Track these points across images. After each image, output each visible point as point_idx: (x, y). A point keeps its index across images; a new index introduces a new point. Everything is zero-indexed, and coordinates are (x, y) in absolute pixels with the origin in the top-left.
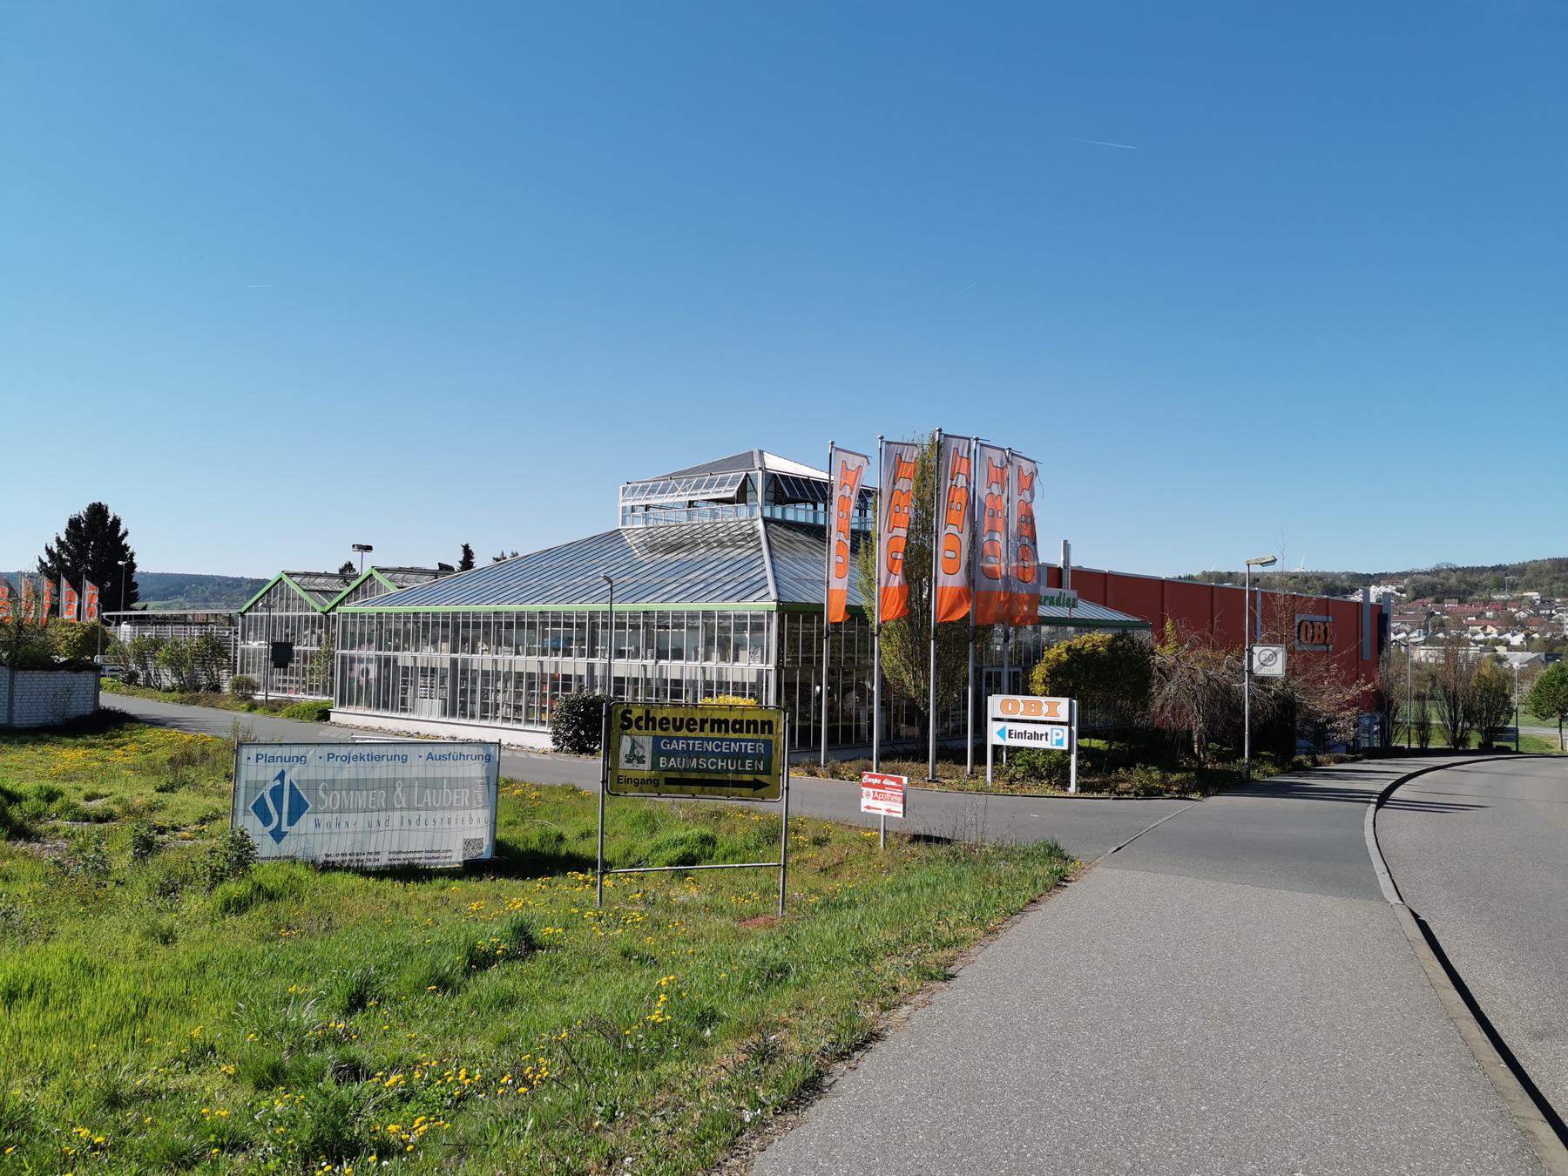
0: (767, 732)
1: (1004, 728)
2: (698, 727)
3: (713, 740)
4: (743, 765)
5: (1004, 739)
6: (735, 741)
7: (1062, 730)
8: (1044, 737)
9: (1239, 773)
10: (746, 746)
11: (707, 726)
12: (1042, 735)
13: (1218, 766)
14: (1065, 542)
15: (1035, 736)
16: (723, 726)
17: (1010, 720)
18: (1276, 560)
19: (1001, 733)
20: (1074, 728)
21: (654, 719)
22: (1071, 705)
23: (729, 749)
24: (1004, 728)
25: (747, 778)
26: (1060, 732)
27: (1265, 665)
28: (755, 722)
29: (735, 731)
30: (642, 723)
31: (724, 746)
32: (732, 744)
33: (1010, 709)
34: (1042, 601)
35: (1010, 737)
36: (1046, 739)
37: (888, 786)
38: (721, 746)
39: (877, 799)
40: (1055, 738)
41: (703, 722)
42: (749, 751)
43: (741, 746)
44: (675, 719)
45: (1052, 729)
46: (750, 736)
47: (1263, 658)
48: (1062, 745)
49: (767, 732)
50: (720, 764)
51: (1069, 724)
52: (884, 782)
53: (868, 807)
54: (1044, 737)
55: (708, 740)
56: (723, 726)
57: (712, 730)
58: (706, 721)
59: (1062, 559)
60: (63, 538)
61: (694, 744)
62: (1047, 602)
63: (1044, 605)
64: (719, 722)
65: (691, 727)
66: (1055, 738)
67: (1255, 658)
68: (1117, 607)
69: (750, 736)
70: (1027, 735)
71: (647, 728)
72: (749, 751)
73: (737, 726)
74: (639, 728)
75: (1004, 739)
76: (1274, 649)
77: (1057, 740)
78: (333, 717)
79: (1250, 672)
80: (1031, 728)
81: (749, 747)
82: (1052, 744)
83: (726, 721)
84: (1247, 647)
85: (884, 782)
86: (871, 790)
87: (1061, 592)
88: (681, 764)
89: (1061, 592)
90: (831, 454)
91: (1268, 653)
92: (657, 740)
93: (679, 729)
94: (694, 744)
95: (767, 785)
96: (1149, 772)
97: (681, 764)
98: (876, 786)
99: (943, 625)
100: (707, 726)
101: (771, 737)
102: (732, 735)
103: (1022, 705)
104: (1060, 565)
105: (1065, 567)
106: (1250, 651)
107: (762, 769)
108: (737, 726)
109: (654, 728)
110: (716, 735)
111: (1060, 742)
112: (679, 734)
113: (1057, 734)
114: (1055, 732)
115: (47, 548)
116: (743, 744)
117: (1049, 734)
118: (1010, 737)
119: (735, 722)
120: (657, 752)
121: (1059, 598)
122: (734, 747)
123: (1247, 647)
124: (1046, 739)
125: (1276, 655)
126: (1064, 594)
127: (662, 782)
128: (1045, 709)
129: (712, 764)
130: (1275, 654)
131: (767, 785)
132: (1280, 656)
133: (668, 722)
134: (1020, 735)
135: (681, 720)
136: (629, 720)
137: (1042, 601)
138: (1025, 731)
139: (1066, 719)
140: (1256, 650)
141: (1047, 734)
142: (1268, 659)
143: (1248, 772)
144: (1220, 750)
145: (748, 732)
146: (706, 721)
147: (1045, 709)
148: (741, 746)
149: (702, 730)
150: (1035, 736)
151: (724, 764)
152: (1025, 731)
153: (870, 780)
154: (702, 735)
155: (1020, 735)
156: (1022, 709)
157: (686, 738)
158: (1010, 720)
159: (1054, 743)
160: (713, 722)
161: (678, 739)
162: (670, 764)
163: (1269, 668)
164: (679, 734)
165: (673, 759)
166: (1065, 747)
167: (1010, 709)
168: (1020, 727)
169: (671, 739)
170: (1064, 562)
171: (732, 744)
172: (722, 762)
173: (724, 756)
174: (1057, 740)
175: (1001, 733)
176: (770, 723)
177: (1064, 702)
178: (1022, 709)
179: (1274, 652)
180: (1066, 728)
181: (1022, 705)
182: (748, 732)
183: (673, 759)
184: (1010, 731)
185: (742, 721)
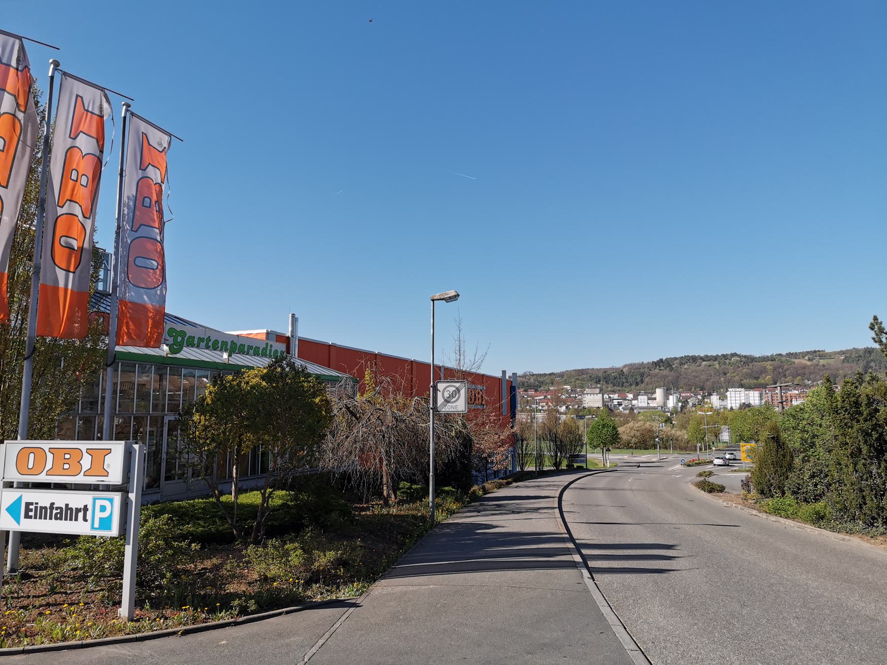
1: (21, 496)
5: (19, 523)
7: (111, 501)
8: (81, 515)
9: (423, 518)
12: (78, 510)
13: (405, 510)
14: (293, 315)
15: (68, 513)
17: (25, 486)
18: (458, 295)
20: (132, 496)
22: (128, 455)
24: (20, 498)
26: (107, 504)
27: (449, 402)
33: (30, 466)
34: (246, 350)
35: (27, 516)
36: (85, 520)
45: (95, 499)
47: (446, 395)
48: (109, 528)
54: (81, 515)
59: (290, 329)
62: (251, 352)
63: (247, 354)
66: (99, 515)
67: (439, 394)
70: (54, 512)
75: (19, 523)
76: (457, 385)
77: (100, 518)
79: (435, 409)
80: (61, 499)
82: (93, 528)
84: (432, 384)
87: (267, 344)
89: (267, 344)
91: (452, 389)
96: (286, 554)
103: (50, 457)
104: (289, 334)
105: (292, 336)
106: (435, 389)
114: (99, 503)
117: (90, 507)
121: (265, 349)
123: (432, 384)
124: (85, 520)
125: (459, 391)
126: (271, 346)
128: (86, 462)
130: (458, 390)
132: (463, 392)
134: (43, 513)
137: (246, 350)
138: (52, 504)
139: (115, 477)
140: (441, 386)
141: (86, 509)
142: (452, 396)
143: (433, 515)
144: (410, 488)
147: (86, 462)
150: (68, 513)
152: (52, 504)
155: (43, 513)
156: (49, 465)
158: (25, 486)
159: (96, 525)
163: (453, 405)
166: (114, 532)
167: (30, 466)
168: (43, 498)
170: (292, 332)
174: (100, 518)
177: (118, 448)
178: (49, 465)
179: (457, 388)
180: (117, 497)
181: (50, 457)
184: (28, 504)
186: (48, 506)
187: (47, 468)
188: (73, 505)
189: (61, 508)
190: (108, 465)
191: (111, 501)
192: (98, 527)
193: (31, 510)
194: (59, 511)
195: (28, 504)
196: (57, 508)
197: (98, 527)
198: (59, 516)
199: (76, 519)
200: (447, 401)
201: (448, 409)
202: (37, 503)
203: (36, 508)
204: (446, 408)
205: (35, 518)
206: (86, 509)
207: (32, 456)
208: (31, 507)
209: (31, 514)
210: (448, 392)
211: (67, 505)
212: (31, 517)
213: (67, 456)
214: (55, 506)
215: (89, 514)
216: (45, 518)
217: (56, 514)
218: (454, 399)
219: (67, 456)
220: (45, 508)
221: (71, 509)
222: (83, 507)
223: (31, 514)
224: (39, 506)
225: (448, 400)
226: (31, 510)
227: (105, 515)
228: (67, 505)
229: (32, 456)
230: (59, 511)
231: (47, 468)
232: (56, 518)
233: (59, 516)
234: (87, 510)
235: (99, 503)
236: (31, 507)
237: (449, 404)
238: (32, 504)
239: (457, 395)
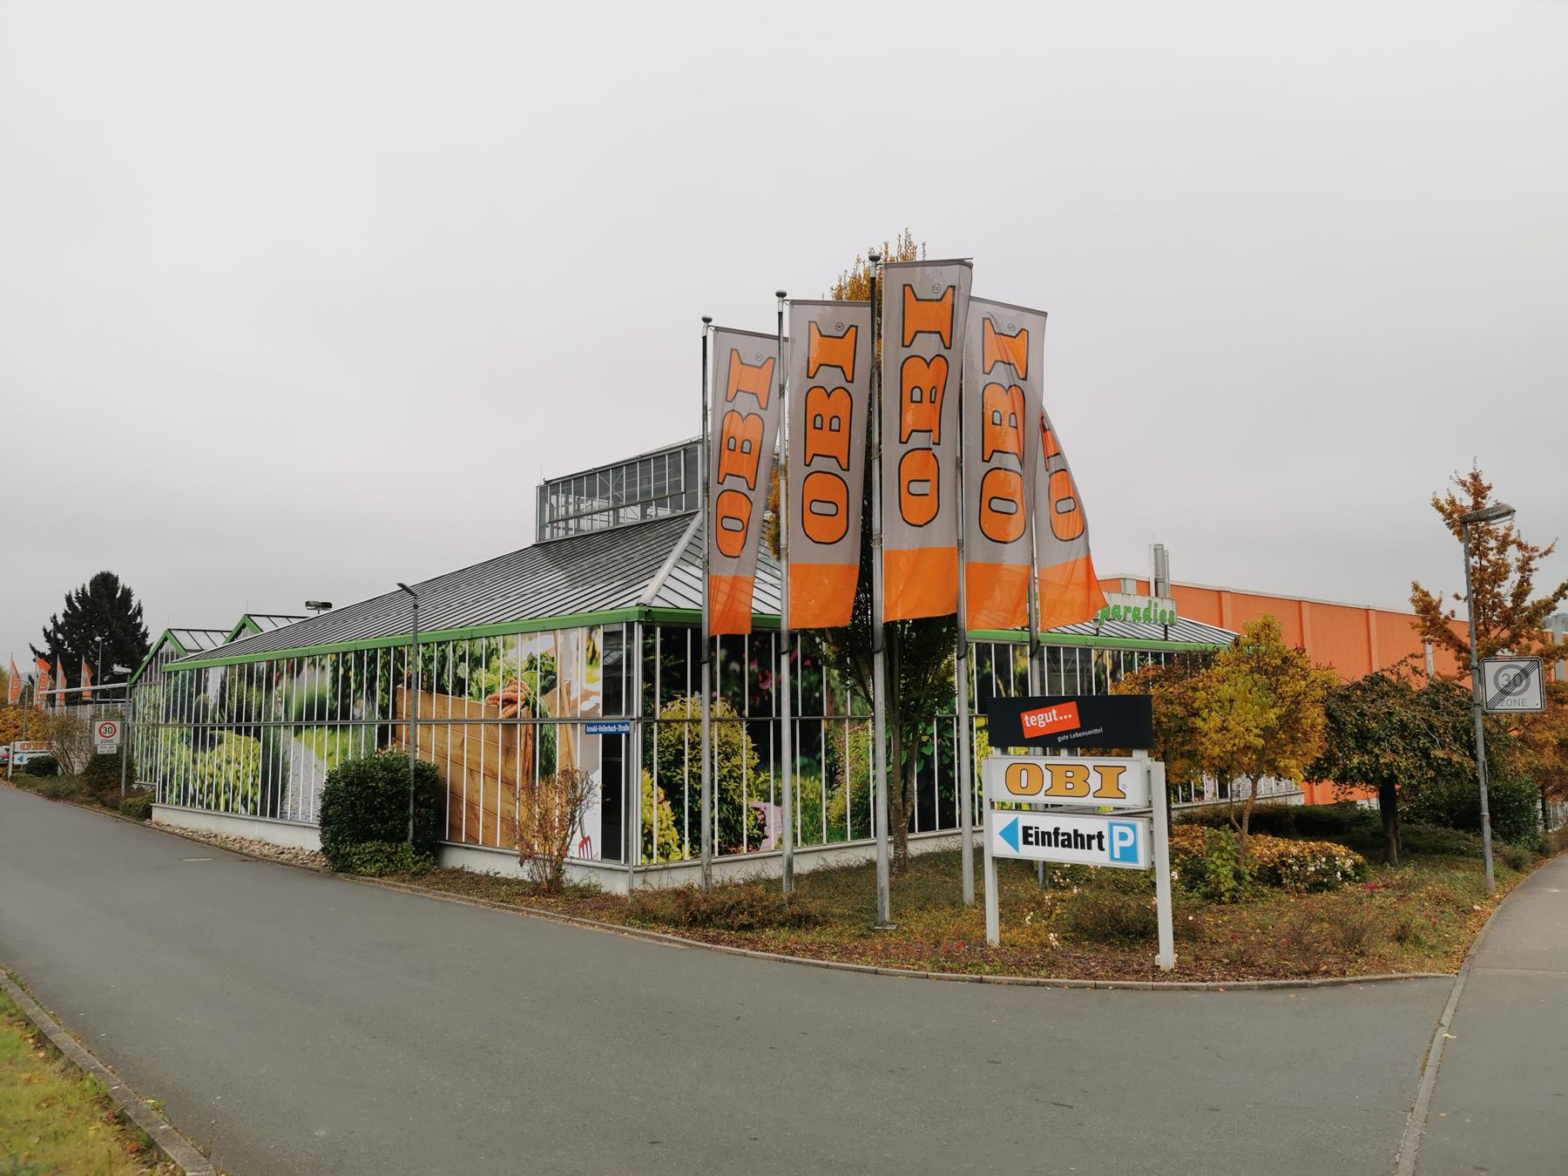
1: (1015, 822)
5: (1018, 851)
7: (1133, 827)
8: (1095, 843)
12: (1090, 838)
15: (1077, 840)
19: (1008, 833)
24: (1015, 822)
27: (1508, 694)
33: (1024, 785)
34: (1122, 614)
35: (1026, 842)
36: (1101, 848)
40: (1118, 844)
45: (1111, 825)
47: (1503, 681)
48: (1135, 860)
51: (1146, 813)
54: (1095, 843)
60: (60, 620)
70: (1060, 838)
75: (1018, 851)
76: (1523, 665)
77: (1122, 849)
78: (158, 814)
82: (1112, 858)
90: (705, 338)
91: (1512, 672)
99: (890, 627)
103: (1047, 774)
111: (1129, 854)
113: (1123, 837)
114: (1117, 830)
115: (45, 630)
118: (1026, 842)
121: (1148, 610)
124: (1101, 848)
126: (1156, 605)
128: (1095, 781)
130: (1525, 673)
134: (1046, 838)
138: (1056, 830)
141: (1100, 836)
142: (1514, 682)
147: (1095, 781)
152: (1056, 830)
155: (1046, 838)
159: (1117, 855)
163: (1517, 698)
167: (1024, 785)
174: (1121, 848)
175: (1008, 833)
179: (1523, 670)
180: (1141, 824)
181: (1047, 774)
184: (1026, 829)
186: (1052, 832)
187: (1044, 789)
188: (1084, 831)
189: (1069, 835)
190: (1124, 786)
191: (1133, 827)
192: (1119, 857)
193: (1031, 835)
194: (1066, 837)
195: (1026, 829)
196: (1063, 834)
197: (1119, 857)
198: (1066, 843)
199: (1090, 847)
200: (1504, 692)
201: (1509, 704)
202: (1036, 828)
203: (1037, 833)
204: (1505, 703)
205: (1037, 844)
207: (1024, 772)
208: (1030, 832)
209: (1030, 839)
210: (1506, 677)
211: (1076, 831)
212: (1031, 843)
213: (1070, 774)
214: (1060, 831)
215: (1105, 842)
216: (1050, 845)
217: (1063, 841)
218: (1517, 689)
219: (1070, 774)
220: (1049, 833)
221: (1082, 836)
222: (1096, 834)
223: (1030, 839)
224: (1040, 831)
225: (1508, 689)
226: (1031, 835)
227: (1128, 843)
228: (1076, 831)
229: (1024, 772)
230: (1066, 837)
231: (1044, 789)
232: (1063, 846)
233: (1066, 843)
234: (1103, 837)
235: (1117, 830)
236: (1030, 832)
237: (1508, 697)
238: (1031, 828)
239: (1524, 682)
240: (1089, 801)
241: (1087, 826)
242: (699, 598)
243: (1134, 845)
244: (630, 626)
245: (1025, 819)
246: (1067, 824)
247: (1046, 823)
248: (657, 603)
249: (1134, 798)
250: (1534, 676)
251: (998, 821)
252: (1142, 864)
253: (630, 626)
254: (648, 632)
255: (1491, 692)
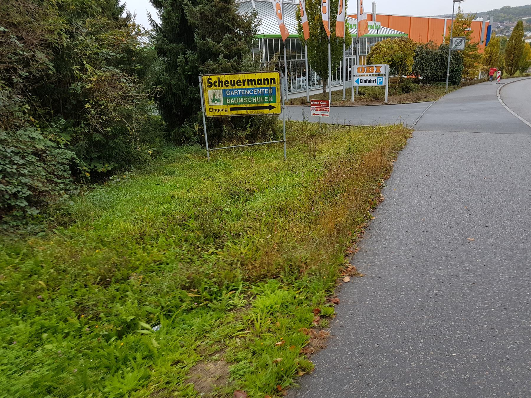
0: (273, 83)
2: (242, 84)
3: (249, 89)
4: (264, 99)
6: (259, 89)
7: (382, 78)
10: (264, 91)
11: (246, 83)
12: (374, 80)
15: (371, 81)
16: (253, 82)
19: (357, 81)
21: (222, 82)
23: (257, 92)
25: (266, 105)
26: (381, 79)
28: (267, 79)
29: (259, 84)
30: (217, 84)
31: (254, 92)
32: (258, 90)
35: (361, 82)
37: (322, 105)
38: (253, 92)
39: (317, 110)
40: (379, 81)
41: (244, 81)
42: (266, 93)
43: (262, 91)
44: (231, 81)
46: (265, 86)
47: (456, 43)
49: (273, 83)
50: (253, 99)
52: (320, 103)
53: (314, 114)
55: (247, 89)
56: (253, 82)
57: (248, 85)
58: (245, 81)
61: (241, 92)
64: (251, 80)
65: (239, 84)
66: (379, 81)
68: (394, 28)
69: (265, 86)
71: (219, 86)
72: (266, 93)
73: (260, 82)
74: (216, 86)
76: (461, 38)
81: (266, 91)
83: (254, 80)
85: (320, 103)
86: (315, 107)
88: (236, 101)
92: (224, 91)
93: (233, 85)
94: (241, 92)
95: (275, 107)
97: (236, 101)
98: (317, 105)
100: (246, 83)
101: (275, 85)
102: (258, 86)
103: (366, 69)
107: (272, 100)
108: (260, 82)
109: (222, 86)
110: (250, 86)
112: (234, 88)
114: (379, 78)
116: (263, 90)
118: (361, 82)
119: (258, 80)
120: (225, 97)
121: (374, 25)
122: (259, 92)
127: (229, 110)
128: (375, 69)
129: (250, 100)
130: (462, 40)
131: (275, 107)
133: (228, 83)
134: (365, 81)
135: (234, 81)
136: (211, 83)
141: (376, 80)
142: (459, 43)
145: (265, 84)
146: (245, 81)
147: (375, 69)
148: (262, 91)
149: (244, 85)
150: (371, 81)
151: (255, 100)
153: (314, 103)
154: (244, 87)
155: (365, 81)
156: (366, 71)
157: (237, 89)
160: (249, 81)
161: (233, 90)
162: (232, 101)
164: (234, 88)
165: (232, 99)
169: (230, 90)
170: (373, 11)
171: (258, 90)
172: (254, 99)
173: (255, 96)
175: (357, 81)
176: (274, 79)
178: (366, 71)
179: (461, 40)
180: (384, 77)
181: (366, 69)
182: (265, 84)
183: (232, 99)
184: (361, 80)
185: (261, 79)
191: (382, 78)
195: (361, 80)
200: (456, 45)
201: (457, 48)
206: (376, 80)
227: (381, 81)
235: (379, 78)
240: (374, 73)
241: (373, 78)
242: (280, 31)
243: (382, 81)
244: (261, 40)
245: (361, 78)
246: (369, 78)
247: (365, 78)
248: (265, 33)
249: (383, 72)
250: (463, 41)
251: (355, 79)
252: (383, 85)
253: (261, 40)
254: (266, 41)
255: (454, 45)
